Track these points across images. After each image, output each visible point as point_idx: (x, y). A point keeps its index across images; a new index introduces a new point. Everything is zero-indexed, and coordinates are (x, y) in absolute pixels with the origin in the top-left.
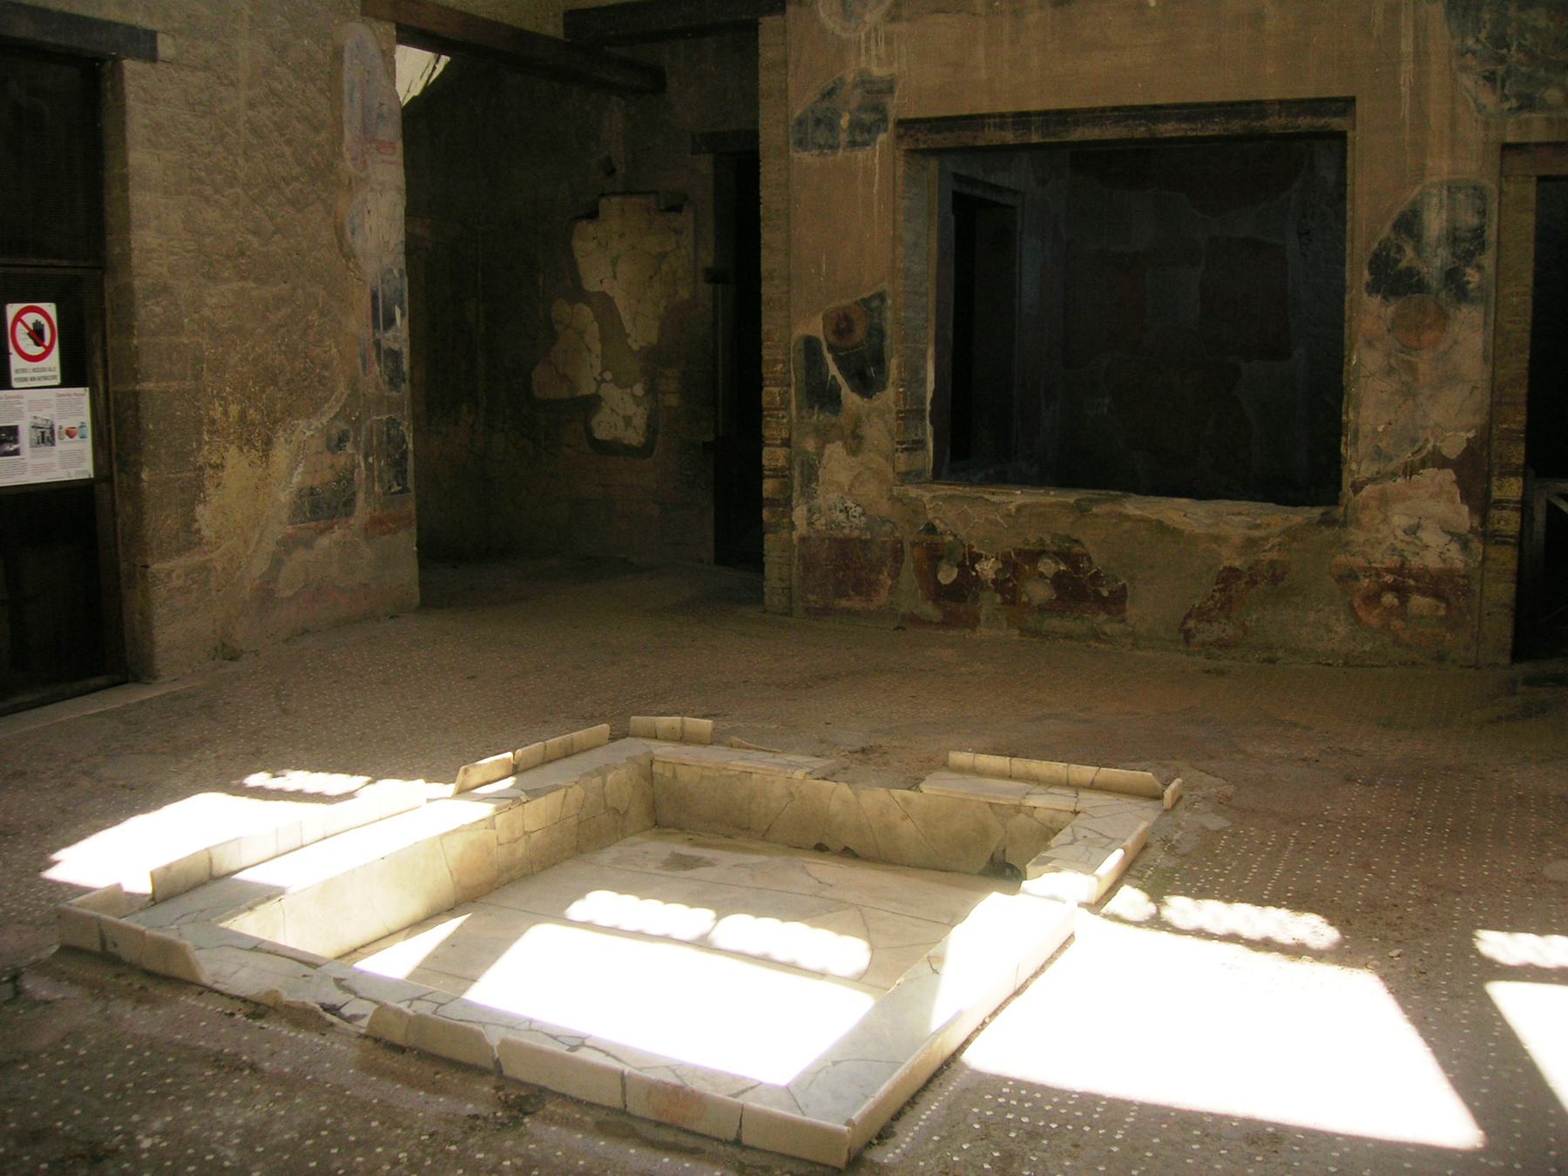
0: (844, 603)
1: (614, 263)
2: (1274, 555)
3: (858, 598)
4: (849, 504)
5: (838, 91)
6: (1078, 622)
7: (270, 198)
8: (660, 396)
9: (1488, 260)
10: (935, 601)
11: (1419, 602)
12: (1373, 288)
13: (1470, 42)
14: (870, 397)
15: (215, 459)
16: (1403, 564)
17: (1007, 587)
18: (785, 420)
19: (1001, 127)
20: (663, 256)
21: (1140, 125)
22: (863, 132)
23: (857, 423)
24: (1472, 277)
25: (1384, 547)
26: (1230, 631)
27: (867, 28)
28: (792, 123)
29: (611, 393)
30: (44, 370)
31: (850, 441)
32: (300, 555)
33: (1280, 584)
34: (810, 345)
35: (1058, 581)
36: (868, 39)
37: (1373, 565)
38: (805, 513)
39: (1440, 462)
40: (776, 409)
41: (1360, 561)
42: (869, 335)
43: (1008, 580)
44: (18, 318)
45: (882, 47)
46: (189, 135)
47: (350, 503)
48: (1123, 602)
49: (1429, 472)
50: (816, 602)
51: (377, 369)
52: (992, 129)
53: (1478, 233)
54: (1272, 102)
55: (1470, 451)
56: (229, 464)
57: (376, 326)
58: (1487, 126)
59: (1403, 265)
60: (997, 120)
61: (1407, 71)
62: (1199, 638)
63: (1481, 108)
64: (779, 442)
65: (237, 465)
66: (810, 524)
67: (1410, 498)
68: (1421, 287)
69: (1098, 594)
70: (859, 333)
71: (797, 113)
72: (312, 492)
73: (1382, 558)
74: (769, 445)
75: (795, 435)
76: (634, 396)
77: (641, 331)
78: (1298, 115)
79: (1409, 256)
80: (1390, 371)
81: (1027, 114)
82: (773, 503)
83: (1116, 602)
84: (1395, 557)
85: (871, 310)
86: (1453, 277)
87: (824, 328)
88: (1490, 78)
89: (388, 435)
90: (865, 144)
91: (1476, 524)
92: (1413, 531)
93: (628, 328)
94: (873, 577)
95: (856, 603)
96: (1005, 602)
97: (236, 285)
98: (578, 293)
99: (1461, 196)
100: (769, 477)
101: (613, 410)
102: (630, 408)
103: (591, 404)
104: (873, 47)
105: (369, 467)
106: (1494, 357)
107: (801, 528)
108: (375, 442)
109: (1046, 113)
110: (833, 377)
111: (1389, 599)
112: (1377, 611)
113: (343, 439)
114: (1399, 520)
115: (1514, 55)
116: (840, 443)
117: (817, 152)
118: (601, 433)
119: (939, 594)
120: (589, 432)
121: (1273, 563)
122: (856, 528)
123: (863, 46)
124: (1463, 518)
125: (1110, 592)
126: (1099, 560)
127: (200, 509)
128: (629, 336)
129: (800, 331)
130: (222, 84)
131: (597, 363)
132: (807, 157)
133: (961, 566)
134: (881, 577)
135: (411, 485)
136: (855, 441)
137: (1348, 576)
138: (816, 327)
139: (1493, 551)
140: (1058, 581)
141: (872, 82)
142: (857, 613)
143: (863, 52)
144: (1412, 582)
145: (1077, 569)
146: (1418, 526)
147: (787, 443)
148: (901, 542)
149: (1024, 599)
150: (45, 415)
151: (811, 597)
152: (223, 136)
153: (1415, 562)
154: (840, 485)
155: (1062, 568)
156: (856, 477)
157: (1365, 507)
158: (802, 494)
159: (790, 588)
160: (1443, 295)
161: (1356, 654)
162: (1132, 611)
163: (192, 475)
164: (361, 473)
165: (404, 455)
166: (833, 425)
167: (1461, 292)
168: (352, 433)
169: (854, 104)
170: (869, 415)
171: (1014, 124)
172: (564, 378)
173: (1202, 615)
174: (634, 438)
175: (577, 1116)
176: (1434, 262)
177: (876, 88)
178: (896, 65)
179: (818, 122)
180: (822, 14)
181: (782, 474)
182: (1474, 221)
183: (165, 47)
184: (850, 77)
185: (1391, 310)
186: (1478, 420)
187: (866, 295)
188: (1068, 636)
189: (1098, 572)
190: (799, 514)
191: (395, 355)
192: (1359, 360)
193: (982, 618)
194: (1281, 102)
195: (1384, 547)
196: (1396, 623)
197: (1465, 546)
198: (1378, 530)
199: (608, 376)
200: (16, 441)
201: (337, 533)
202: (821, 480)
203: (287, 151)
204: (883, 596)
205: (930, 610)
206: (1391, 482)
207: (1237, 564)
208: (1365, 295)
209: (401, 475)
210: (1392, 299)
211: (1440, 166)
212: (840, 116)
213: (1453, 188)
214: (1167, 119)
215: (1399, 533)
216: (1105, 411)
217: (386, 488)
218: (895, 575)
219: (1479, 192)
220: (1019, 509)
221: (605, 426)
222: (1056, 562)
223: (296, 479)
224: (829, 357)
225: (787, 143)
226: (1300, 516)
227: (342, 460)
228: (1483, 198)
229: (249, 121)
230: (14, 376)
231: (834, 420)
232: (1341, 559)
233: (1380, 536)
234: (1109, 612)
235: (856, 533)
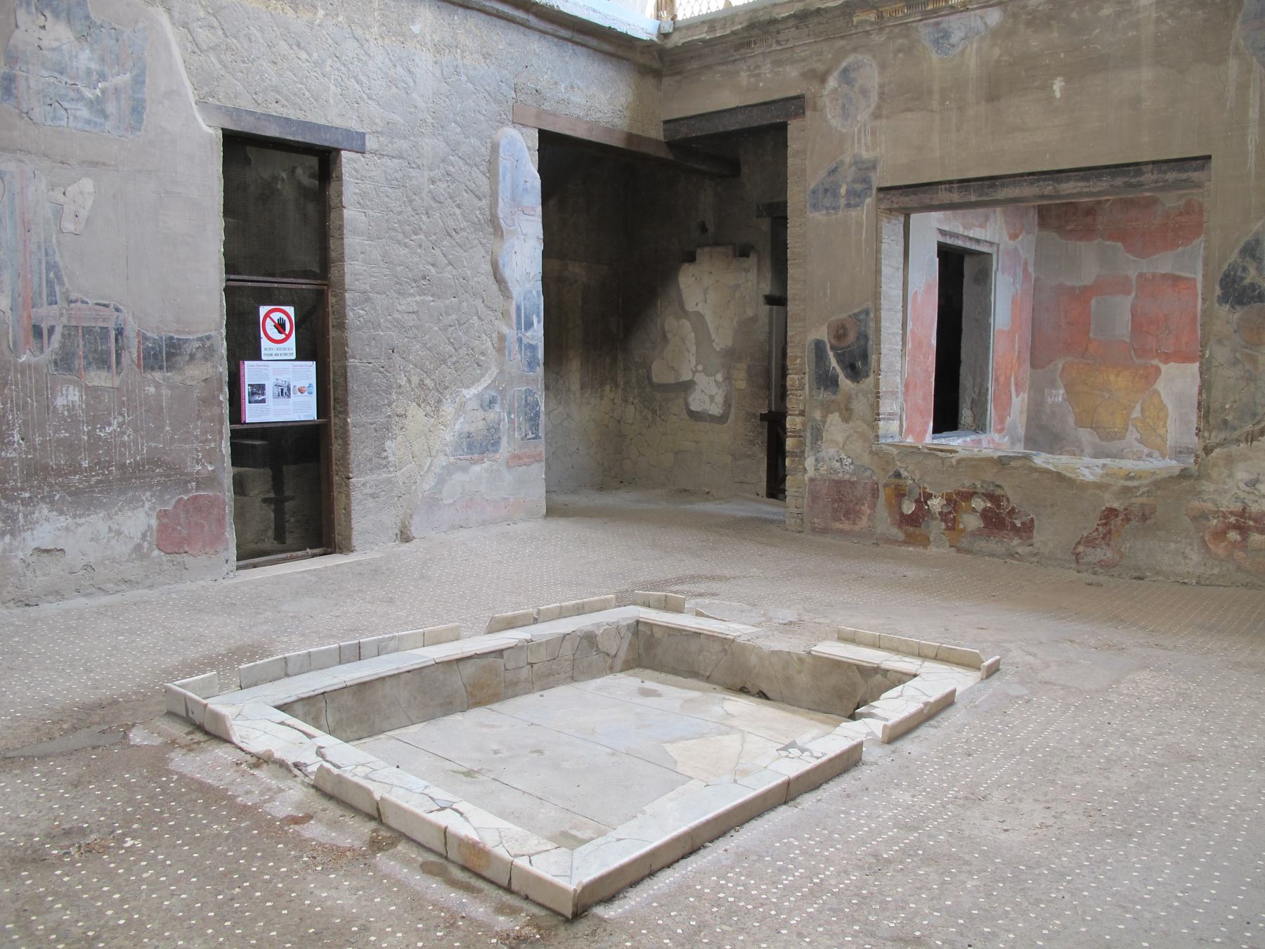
0: (838, 525)
1: (705, 292)
2: (1144, 500)
3: (847, 522)
4: (843, 456)
5: (839, 170)
6: (999, 544)
7: (444, 243)
8: (733, 382)
10: (900, 527)
12: (1223, 299)
14: (858, 382)
15: (400, 411)
16: (1244, 509)
18: (802, 398)
20: (737, 287)
21: (1048, 185)
22: (855, 197)
23: (849, 398)
25: (1229, 496)
26: (1109, 554)
27: (859, 125)
29: (701, 379)
30: (285, 349)
31: (844, 412)
32: (459, 477)
33: (1148, 522)
34: (819, 346)
35: (985, 514)
36: (859, 132)
37: (1221, 509)
38: (813, 461)
40: (796, 390)
41: (1210, 506)
42: (858, 338)
43: (950, 513)
44: (267, 315)
45: (869, 137)
46: (387, 199)
47: (496, 444)
48: (1032, 531)
50: (819, 524)
51: (518, 356)
52: (944, 192)
56: (410, 414)
57: (519, 328)
59: (1247, 281)
60: (947, 186)
64: (797, 413)
65: (416, 415)
66: (817, 469)
67: (1250, 458)
69: (1014, 525)
70: (851, 337)
71: (812, 186)
72: (469, 435)
73: (1228, 504)
74: (791, 415)
75: (807, 406)
76: (715, 381)
77: (722, 338)
78: (1165, 173)
80: (1236, 362)
82: (794, 454)
83: (1027, 529)
84: (1238, 504)
85: (859, 321)
87: (828, 333)
89: (526, 401)
90: (856, 205)
93: (713, 337)
94: (858, 507)
95: (846, 526)
96: (948, 528)
97: (418, 298)
98: (683, 312)
100: (790, 436)
101: (702, 391)
102: (714, 390)
103: (687, 386)
104: (863, 138)
105: (511, 421)
107: (811, 472)
108: (516, 405)
110: (834, 368)
111: (1234, 535)
112: (1223, 544)
113: (492, 402)
114: (1242, 474)
116: (837, 414)
117: (824, 212)
118: (694, 407)
120: (687, 405)
121: (1142, 504)
122: (847, 473)
123: (856, 138)
125: (1022, 523)
126: (1014, 501)
127: (388, 443)
128: (714, 341)
130: (411, 167)
131: (693, 363)
132: (819, 216)
133: (917, 501)
134: (863, 508)
135: (541, 434)
137: (1201, 517)
138: (822, 333)
140: (985, 514)
141: (862, 162)
143: (856, 141)
144: (1251, 523)
145: (999, 507)
146: (1257, 481)
147: (802, 413)
148: (877, 484)
149: (961, 526)
150: (283, 378)
151: (815, 520)
152: (411, 201)
154: (837, 443)
155: (989, 505)
156: (848, 437)
157: (1215, 465)
158: (812, 449)
161: (1205, 576)
162: (1037, 537)
163: (384, 420)
164: (505, 426)
165: (537, 414)
166: (833, 401)
168: (499, 398)
169: (849, 179)
170: (856, 396)
171: (958, 188)
172: (672, 368)
173: (1089, 542)
174: (716, 410)
175: (414, 856)
177: (865, 166)
178: (878, 149)
179: (826, 190)
180: (829, 117)
181: (799, 435)
183: (371, 143)
185: (1237, 315)
187: (856, 311)
188: (992, 555)
189: (1013, 509)
190: (809, 462)
191: (533, 348)
192: (1211, 353)
193: (931, 539)
194: (1154, 162)
195: (1229, 496)
196: (1239, 554)
198: (1224, 483)
199: (700, 368)
200: (263, 394)
201: (487, 464)
202: (824, 440)
203: (458, 211)
204: (864, 522)
205: (895, 532)
206: (1235, 447)
207: (1115, 505)
208: (1217, 305)
209: (535, 426)
210: (1238, 307)
212: (841, 186)
214: (1068, 180)
215: (1242, 485)
216: (1060, 399)
217: (524, 435)
218: (873, 506)
221: (698, 401)
222: (984, 501)
223: (457, 427)
224: (831, 354)
225: (805, 206)
227: (491, 415)
229: (430, 192)
230: (263, 352)
231: (833, 397)
232: (1196, 504)
233: (1226, 487)
235: (847, 477)
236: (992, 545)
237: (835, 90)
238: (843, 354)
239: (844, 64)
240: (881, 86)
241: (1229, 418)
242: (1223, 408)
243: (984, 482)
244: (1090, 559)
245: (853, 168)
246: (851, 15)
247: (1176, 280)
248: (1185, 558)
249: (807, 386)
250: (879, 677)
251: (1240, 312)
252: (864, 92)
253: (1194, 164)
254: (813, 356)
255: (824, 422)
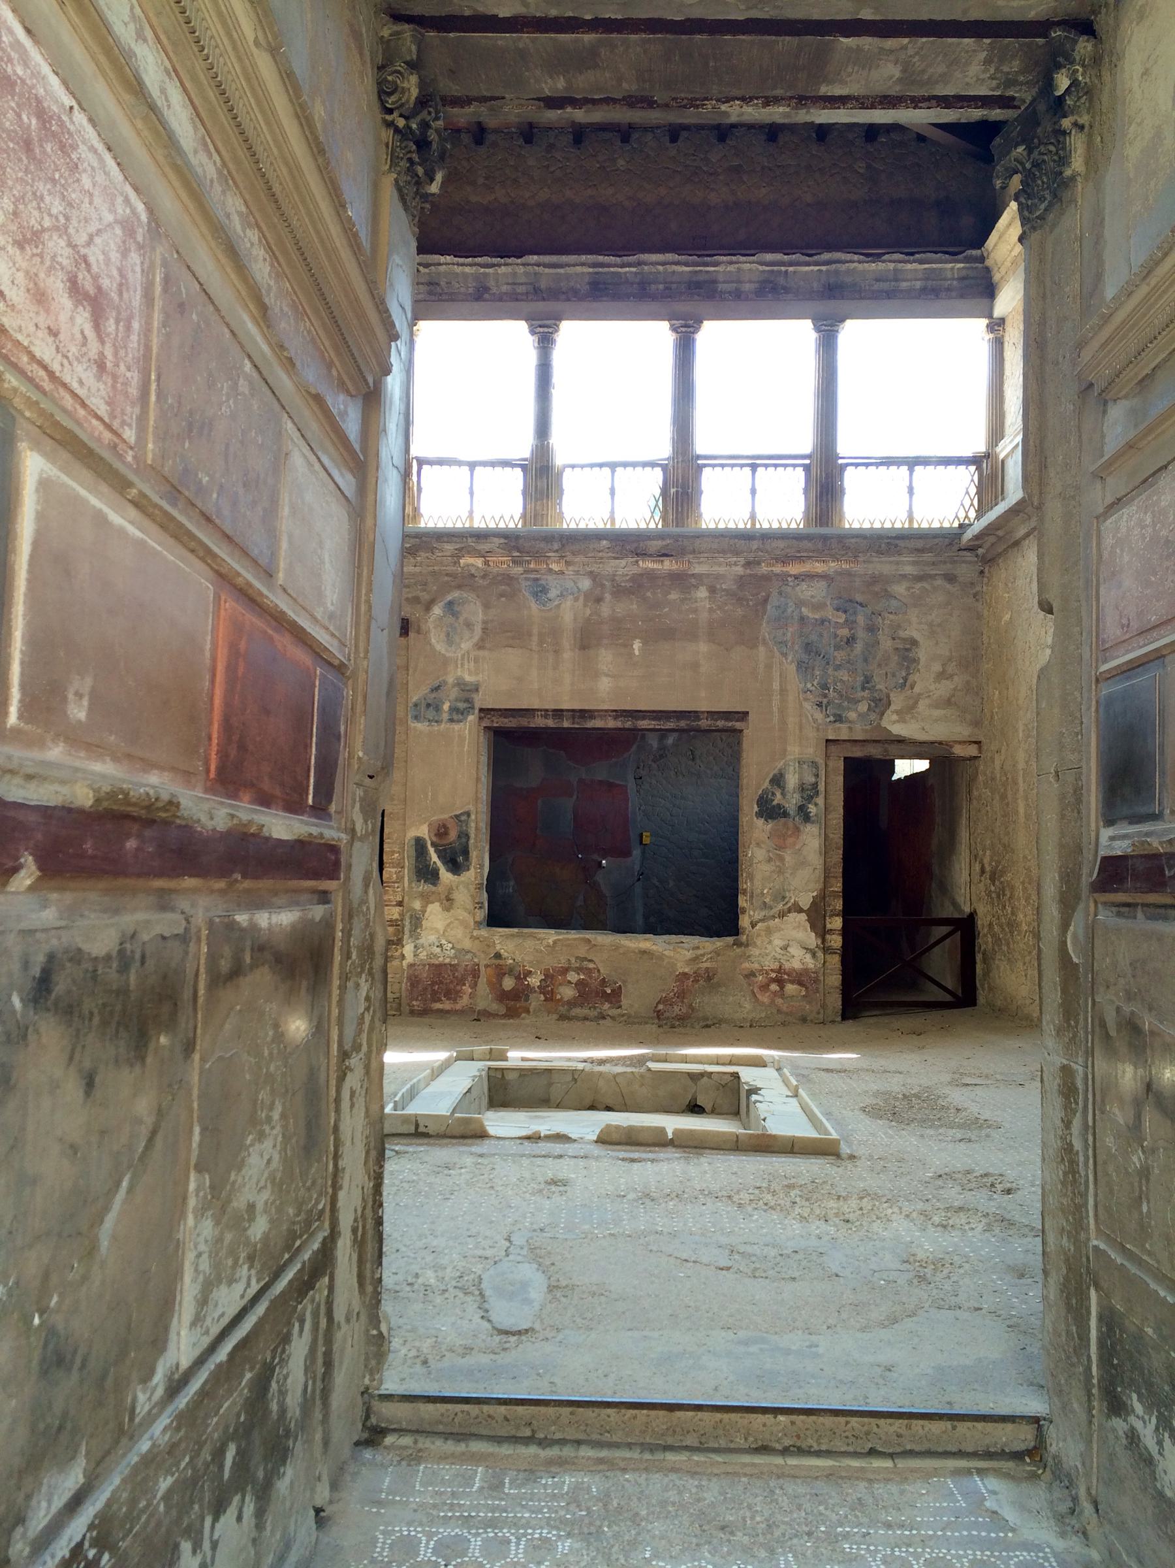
0: (438, 1006)
2: (708, 965)
4: (443, 942)
9: (820, 800)
11: (791, 988)
12: (759, 815)
13: (809, 685)
17: (548, 992)
19: (546, 717)
22: (458, 714)
23: (450, 890)
24: (812, 809)
28: (410, 705)
34: (419, 844)
36: (463, 659)
39: (800, 911)
41: (756, 966)
42: (459, 837)
45: (472, 664)
49: (793, 915)
53: (815, 786)
54: (703, 712)
55: (814, 904)
58: (818, 730)
59: (775, 803)
61: (776, 699)
62: (666, 1015)
63: (815, 721)
68: (785, 814)
70: (453, 835)
71: (415, 699)
75: (406, 898)
79: (778, 799)
80: (770, 860)
81: (562, 710)
86: (802, 809)
88: (820, 705)
91: (819, 942)
92: (785, 948)
94: (458, 988)
95: (447, 1005)
99: (805, 766)
106: (826, 852)
107: (410, 958)
109: (573, 711)
111: (774, 987)
114: (778, 942)
115: (832, 694)
116: (437, 904)
119: (503, 996)
121: (707, 969)
124: (812, 940)
129: (413, 833)
133: (518, 978)
136: (448, 901)
138: (423, 831)
139: (828, 957)
140: (580, 984)
141: (465, 684)
142: (448, 1012)
147: (400, 904)
149: (558, 997)
153: (787, 966)
154: (437, 931)
156: (448, 925)
157: (758, 935)
158: (411, 936)
159: (399, 998)
160: (797, 819)
162: (625, 1002)
166: (433, 893)
167: (807, 818)
176: (792, 802)
179: (428, 705)
180: (433, 641)
182: (813, 780)
184: (451, 680)
186: (820, 886)
190: (408, 949)
196: (779, 1001)
197: (814, 955)
204: (464, 1001)
205: (495, 1007)
207: (686, 970)
211: (794, 750)
213: (800, 763)
214: (644, 718)
215: (778, 949)
218: (474, 986)
219: (814, 764)
220: (555, 942)
224: (432, 850)
226: (719, 943)
228: (817, 768)
231: (433, 888)
232: (746, 965)
234: (611, 1003)
235: (447, 961)
236: (584, 1011)
237: (441, 619)
238: (445, 850)
239: (449, 598)
240: (484, 622)
241: (767, 900)
242: (762, 893)
243: (577, 958)
244: (666, 1015)
245: (456, 689)
246: (460, 557)
247: (611, 786)
248: (741, 1007)
249: (406, 878)
250: (705, 1078)
251: (770, 826)
252: (469, 625)
253: (737, 716)
254: (413, 853)
255: (424, 912)
